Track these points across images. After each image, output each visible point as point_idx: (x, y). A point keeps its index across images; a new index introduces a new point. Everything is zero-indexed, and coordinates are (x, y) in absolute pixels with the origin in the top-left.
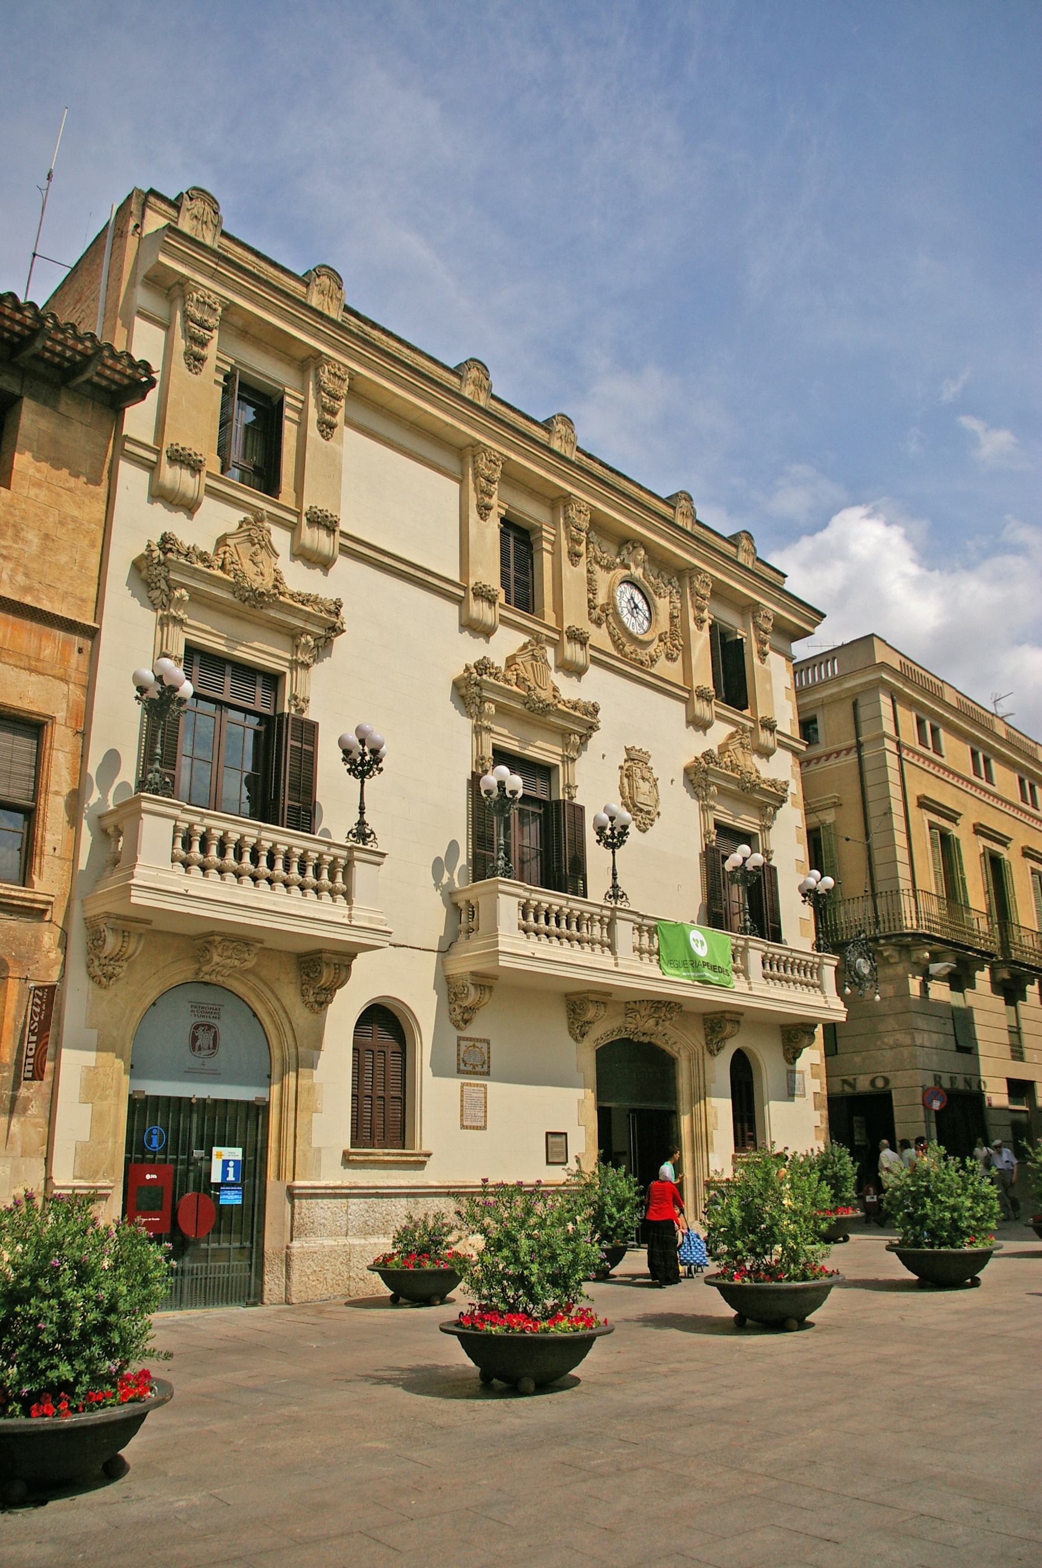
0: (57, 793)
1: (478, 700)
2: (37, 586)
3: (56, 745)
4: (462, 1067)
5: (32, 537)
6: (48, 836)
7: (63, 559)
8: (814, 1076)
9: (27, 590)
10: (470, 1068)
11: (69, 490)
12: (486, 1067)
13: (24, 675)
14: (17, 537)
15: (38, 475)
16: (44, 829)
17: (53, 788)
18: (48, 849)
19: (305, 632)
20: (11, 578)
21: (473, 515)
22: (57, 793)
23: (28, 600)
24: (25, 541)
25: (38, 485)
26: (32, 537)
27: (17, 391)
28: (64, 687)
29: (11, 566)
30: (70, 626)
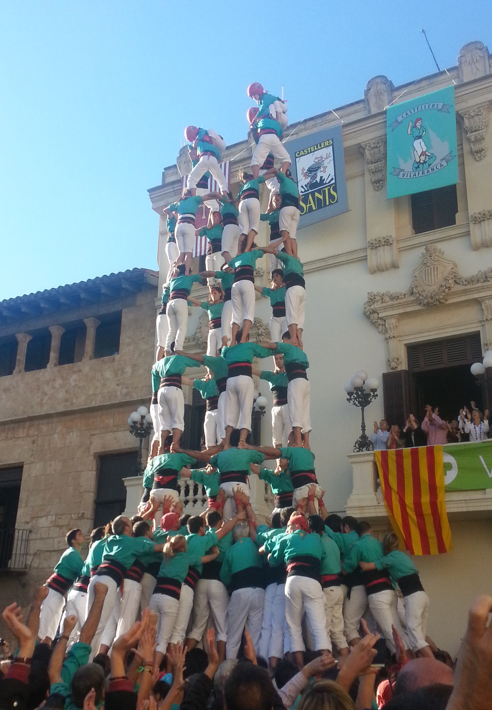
1: (380, 322)
2: (131, 390)
5: (128, 370)
7: (141, 372)
9: (127, 394)
11: (143, 338)
14: (123, 372)
15: (129, 340)
20: (121, 392)
23: (128, 399)
26: (128, 370)
29: (121, 387)
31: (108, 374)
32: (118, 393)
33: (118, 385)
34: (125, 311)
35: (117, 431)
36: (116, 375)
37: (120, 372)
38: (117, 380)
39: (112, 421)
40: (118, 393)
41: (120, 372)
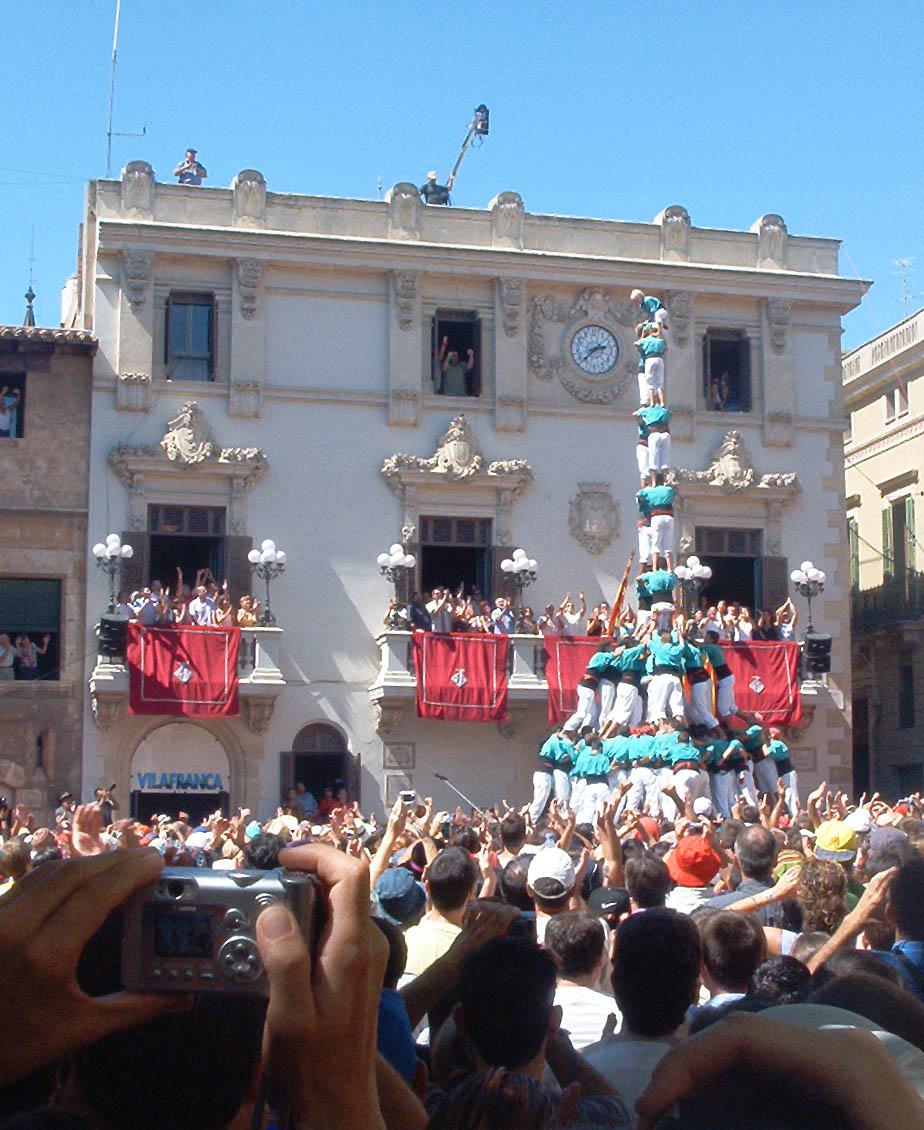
0: (71, 620)
3: (68, 591)
4: (388, 764)
5: (42, 464)
6: (67, 648)
7: (63, 471)
8: (830, 752)
10: (396, 765)
12: (411, 764)
13: (46, 554)
16: (65, 644)
17: (68, 617)
18: (68, 654)
19: (236, 477)
20: (31, 494)
21: (395, 330)
22: (71, 620)
23: (42, 507)
24: (38, 468)
25: (42, 428)
26: (42, 464)
27: (21, 368)
28: (70, 553)
30: (70, 515)
31: (7, 464)
32: (27, 495)
33: (24, 482)
34: (31, 377)
35: (28, 548)
36: (21, 468)
37: (27, 466)
38: (25, 477)
39: (18, 532)
40: (27, 495)
41: (27, 466)
